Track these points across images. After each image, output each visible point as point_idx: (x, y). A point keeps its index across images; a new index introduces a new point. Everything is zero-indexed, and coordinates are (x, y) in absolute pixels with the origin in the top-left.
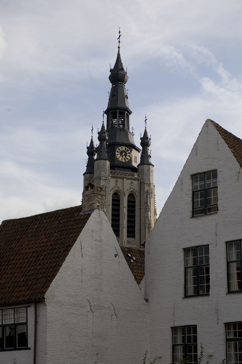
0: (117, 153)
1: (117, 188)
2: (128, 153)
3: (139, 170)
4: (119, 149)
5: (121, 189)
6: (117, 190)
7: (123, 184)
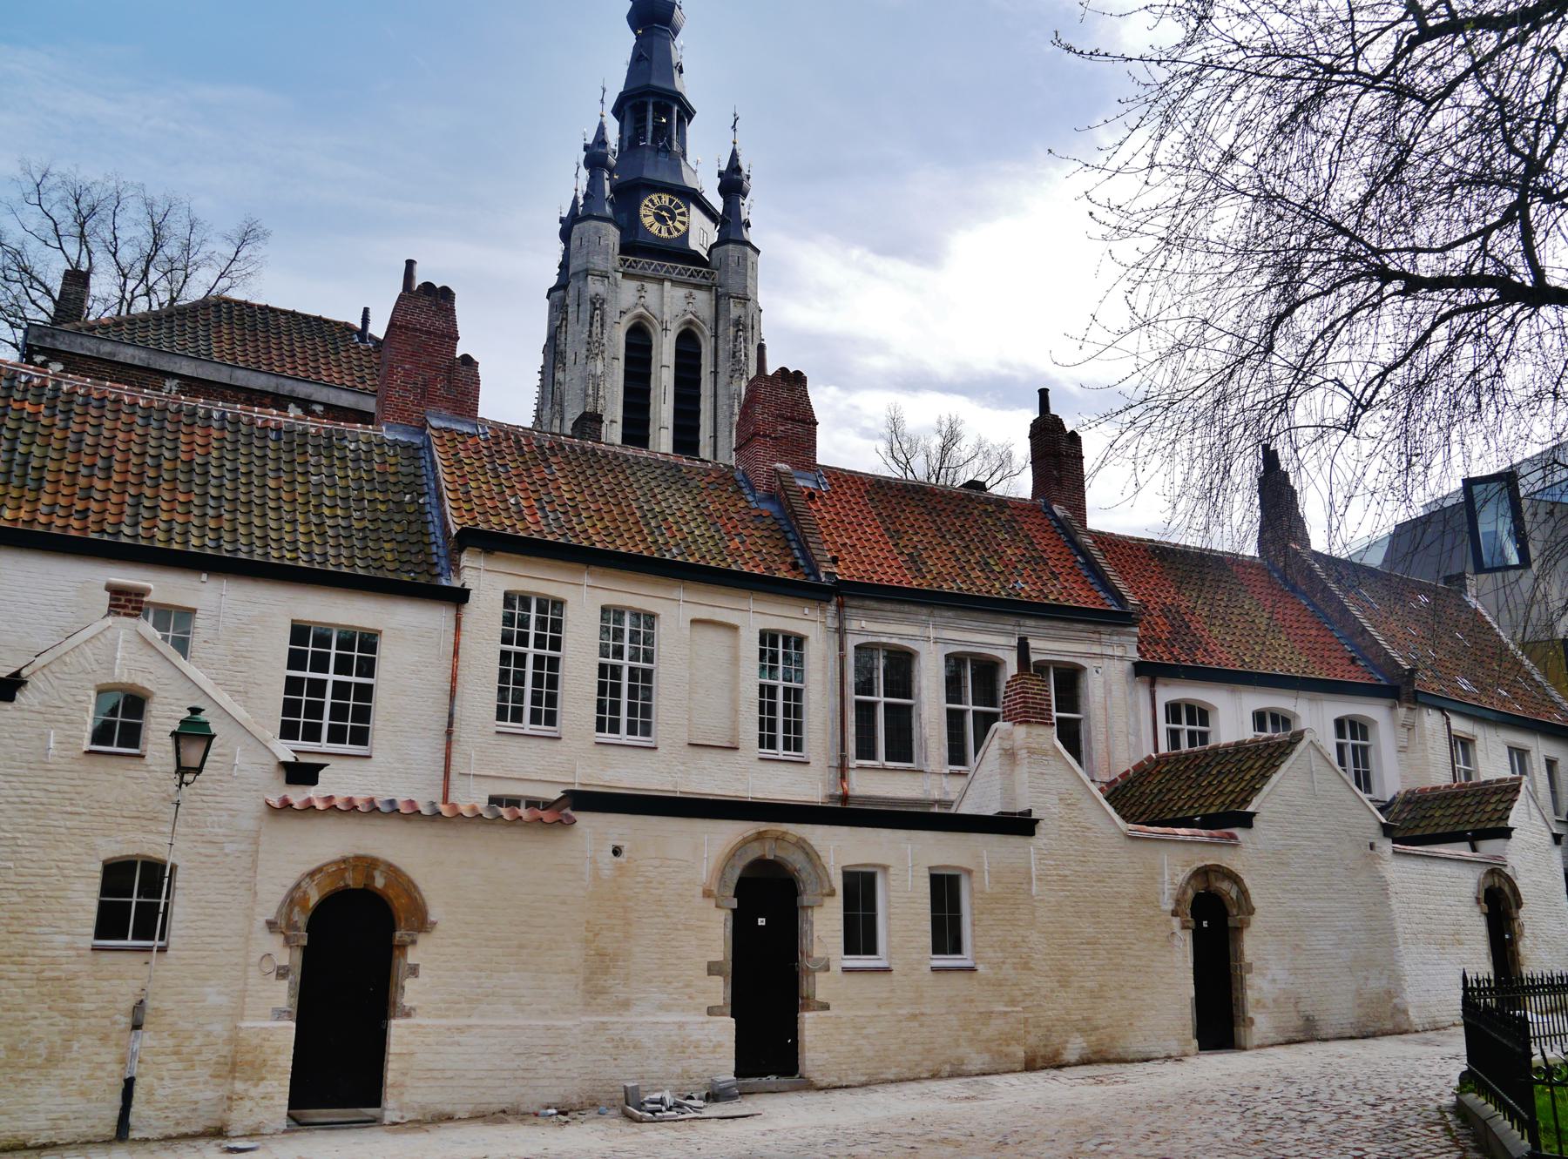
0: (643, 211)
1: (642, 310)
2: (680, 214)
3: (715, 263)
4: (651, 201)
5: (658, 315)
6: (641, 316)
7: (662, 297)
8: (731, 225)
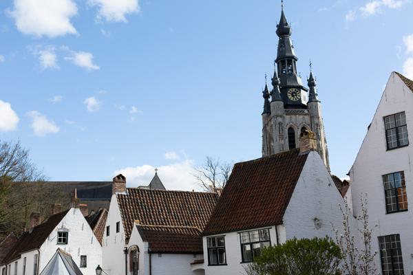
3: (309, 107)
8: (312, 96)
